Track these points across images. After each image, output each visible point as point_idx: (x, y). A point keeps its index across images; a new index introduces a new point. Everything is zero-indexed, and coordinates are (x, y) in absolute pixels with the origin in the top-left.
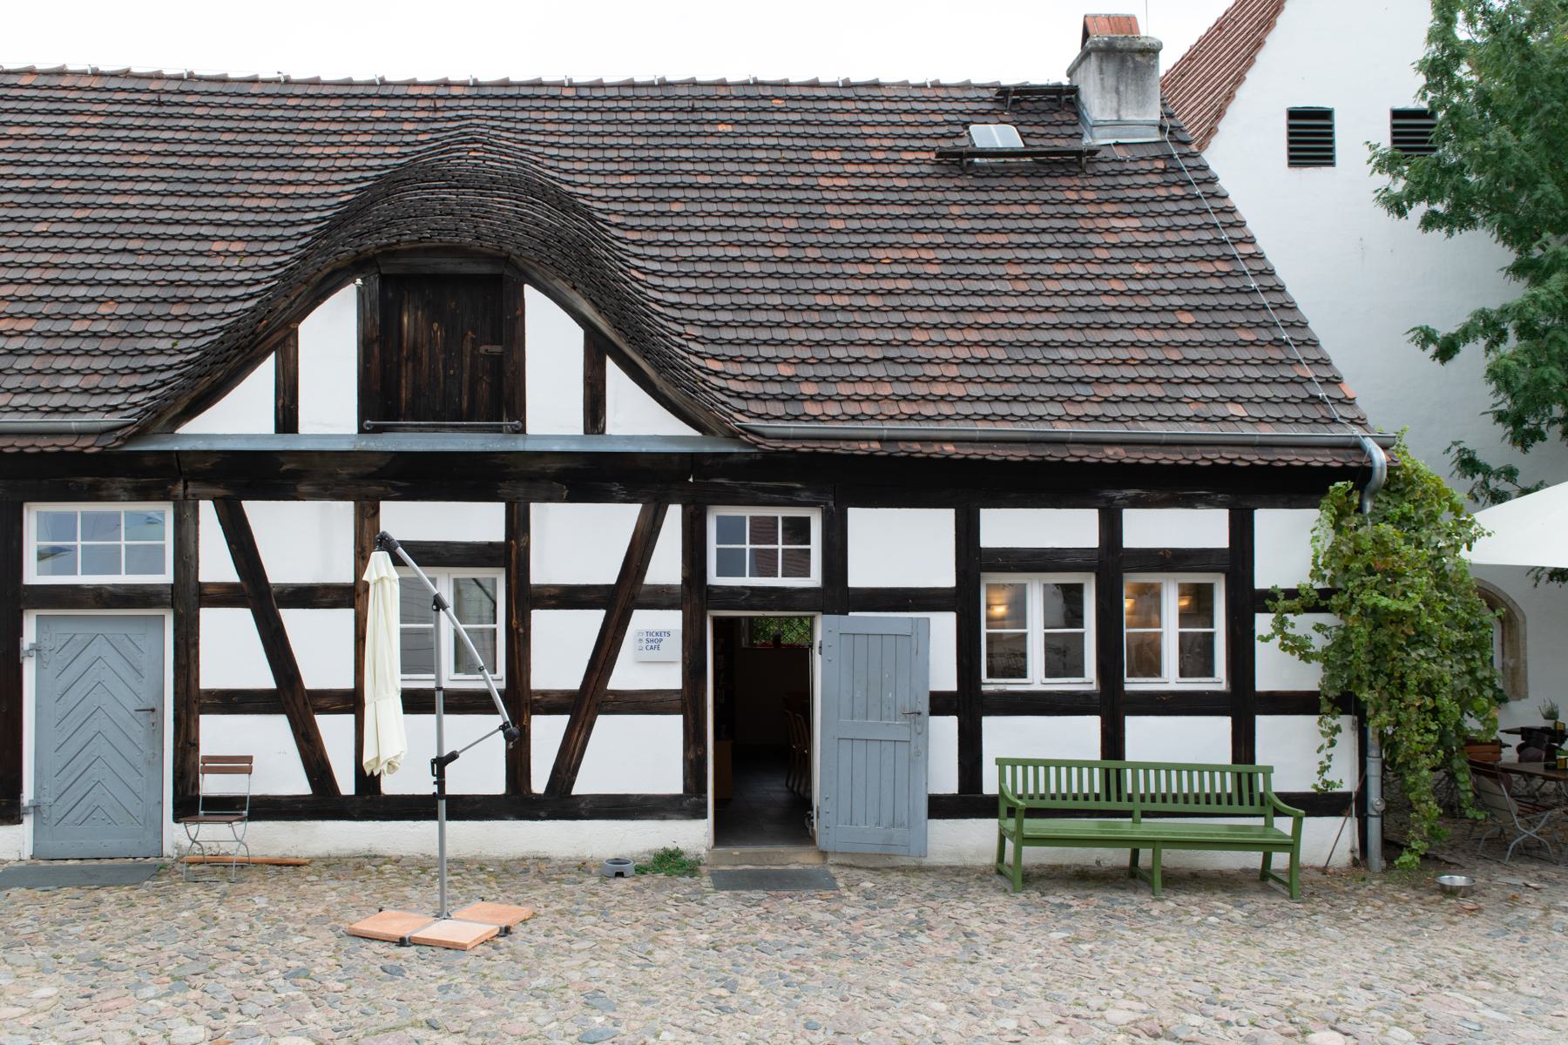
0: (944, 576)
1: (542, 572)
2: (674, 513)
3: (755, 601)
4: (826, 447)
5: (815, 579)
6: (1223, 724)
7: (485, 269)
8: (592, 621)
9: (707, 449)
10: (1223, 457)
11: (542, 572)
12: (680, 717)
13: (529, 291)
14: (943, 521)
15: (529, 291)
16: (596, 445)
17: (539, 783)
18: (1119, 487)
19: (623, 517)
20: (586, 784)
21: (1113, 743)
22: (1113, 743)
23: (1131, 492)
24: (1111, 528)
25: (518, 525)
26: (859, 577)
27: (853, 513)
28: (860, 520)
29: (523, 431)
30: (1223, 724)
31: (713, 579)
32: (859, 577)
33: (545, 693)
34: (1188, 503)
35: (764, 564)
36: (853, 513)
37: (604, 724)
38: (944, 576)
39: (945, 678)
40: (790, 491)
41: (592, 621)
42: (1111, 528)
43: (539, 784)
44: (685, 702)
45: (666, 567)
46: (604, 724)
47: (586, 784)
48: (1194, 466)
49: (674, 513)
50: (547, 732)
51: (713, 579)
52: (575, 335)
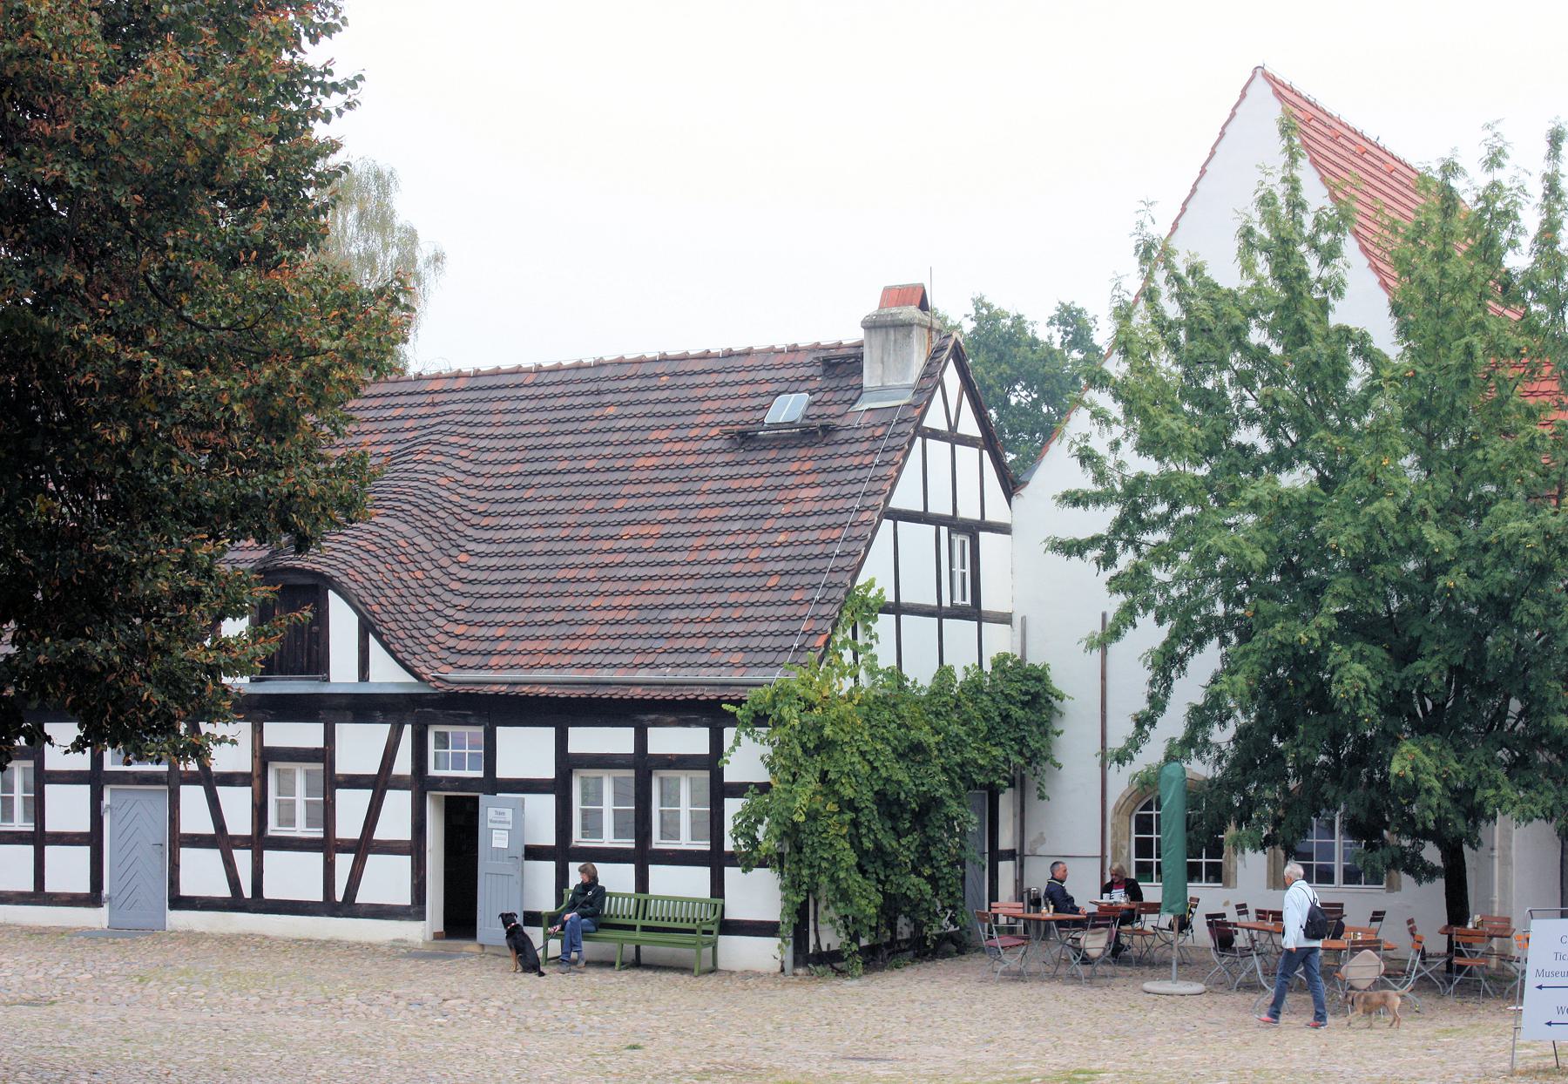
0: (550, 774)
1: (342, 767)
2: (408, 729)
3: (448, 785)
4: (473, 689)
5: (480, 774)
6: (705, 872)
7: (309, 581)
8: (366, 795)
9: (415, 691)
10: (690, 694)
11: (342, 767)
12: (409, 858)
13: (331, 593)
14: (544, 737)
15: (331, 593)
16: (364, 689)
17: (339, 896)
18: (646, 714)
19: (381, 731)
20: (362, 898)
21: (642, 882)
22: (642, 882)
23: (653, 717)
24: (641, 740)
25: (329, 737)
26: (502, 772)
27: (500, 730)
28: (507, 736)
29: (328, 680)
30: (705, 872)
31: (432, 771)
32: (502, 772)
33: (342, 841)
34: (685, 723)
35: (459, 765)
36: (500, 730)
37: (371, 858)
38: (550, 774)
39: (548, 838)
40: (466, 716)
41: (366, 795)
42: (641, 740)
43: (339, 896)
44: (415, 848)
45: (403, 765)
46: (371, 858)
47: (363, 897)
48: (674, 700)
49: (408, 729)
50: (344, 862)
51: (432, 771)
52: (354, 619)
